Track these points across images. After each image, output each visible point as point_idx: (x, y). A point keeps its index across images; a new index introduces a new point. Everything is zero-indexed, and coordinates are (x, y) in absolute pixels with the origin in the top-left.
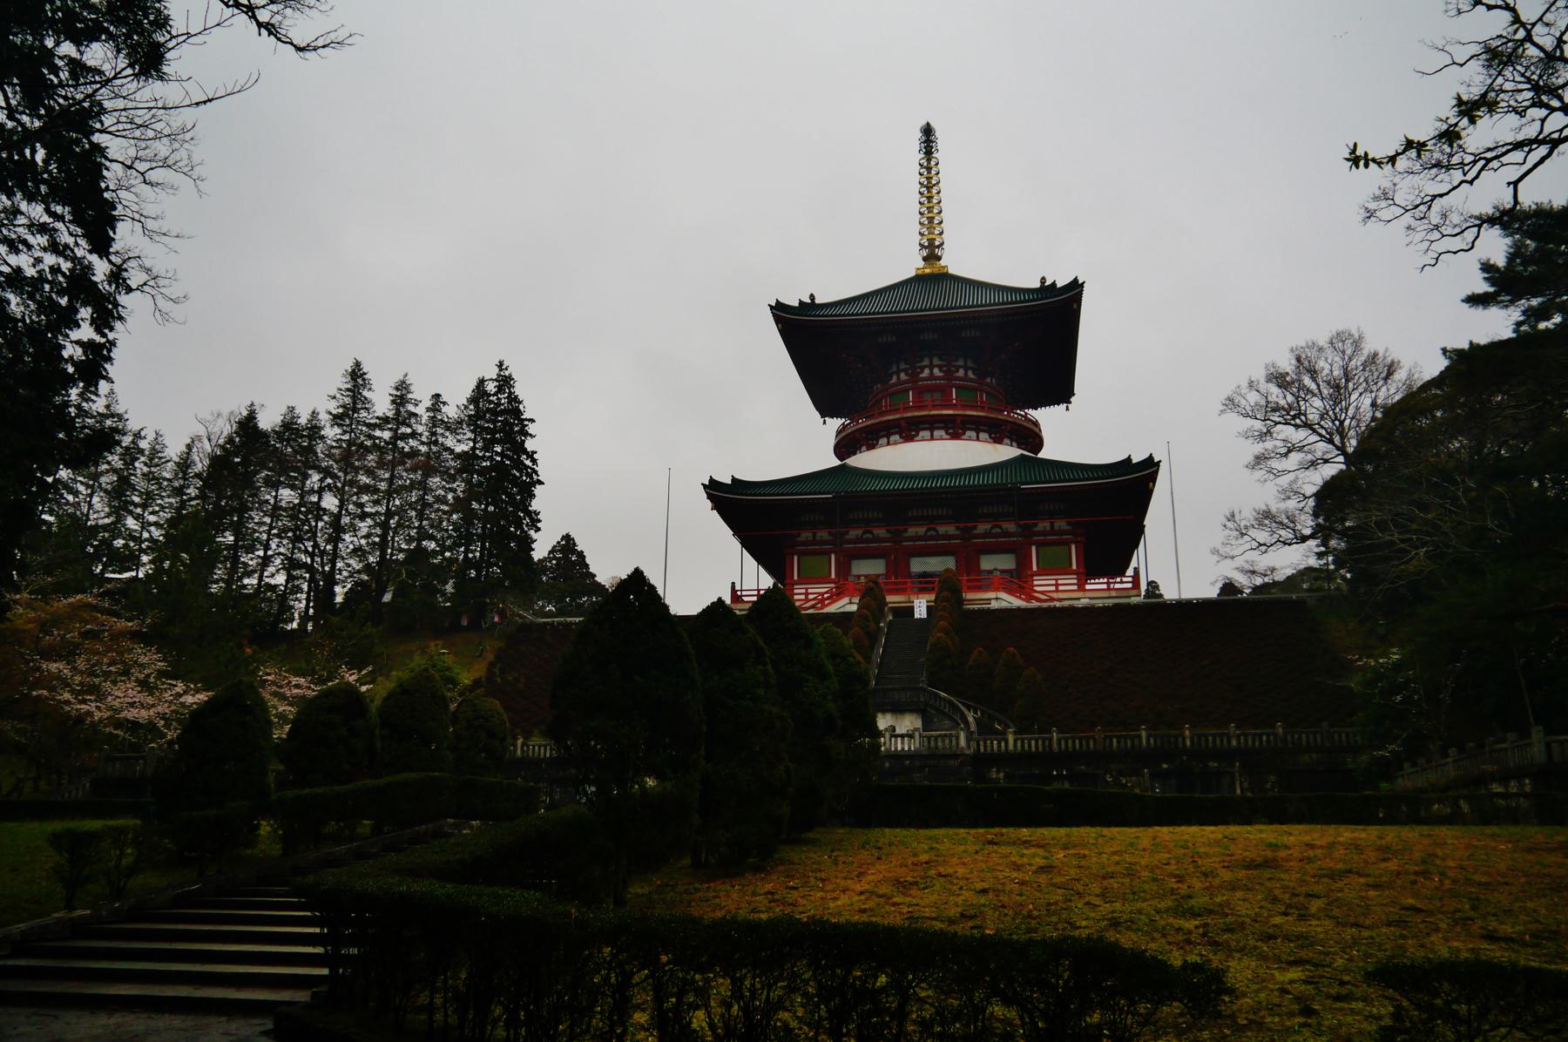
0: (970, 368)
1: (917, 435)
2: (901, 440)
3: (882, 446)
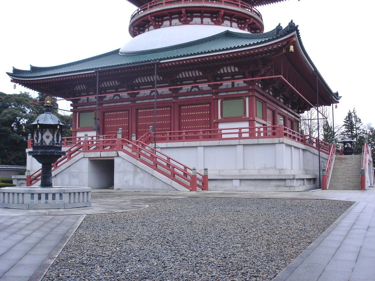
1: (192, 20)
2: (181, 23)
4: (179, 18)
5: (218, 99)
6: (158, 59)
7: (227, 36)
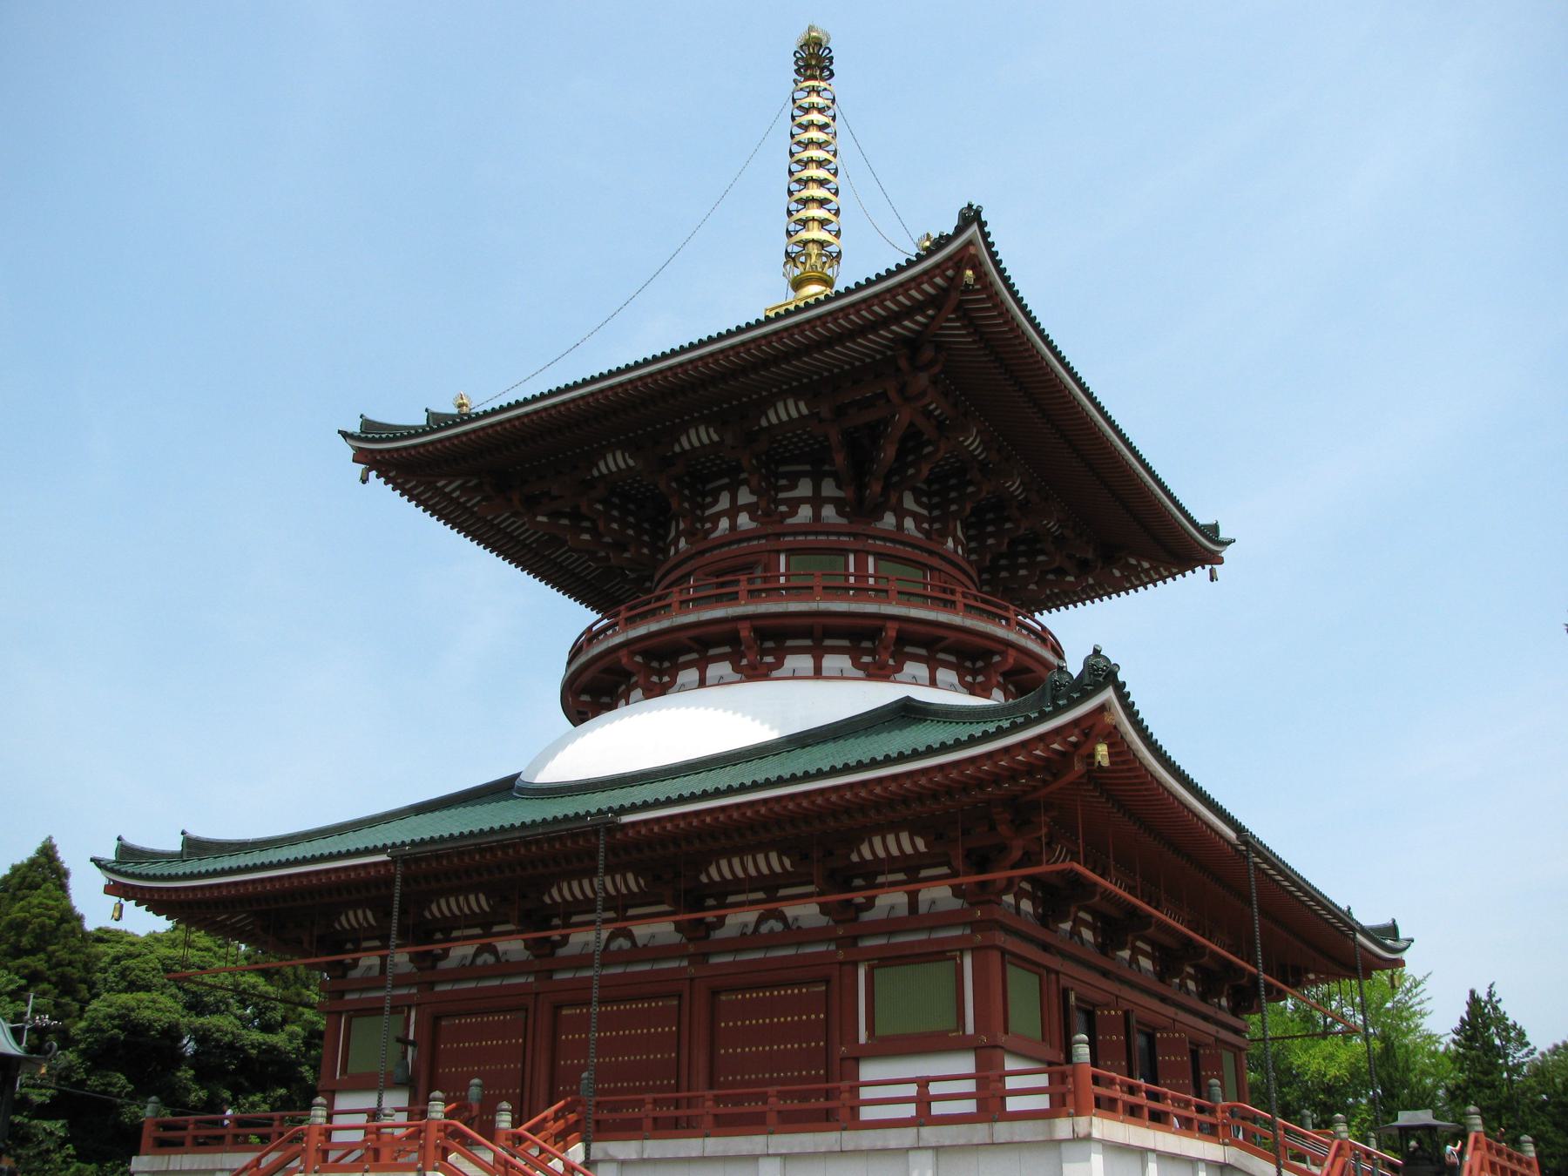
0: (915, 516)
1: (779, 664)
3: (683, 688)
4: (734, 659)
5: (855, 964)
6: (610, 809)
7: (903, 717)
